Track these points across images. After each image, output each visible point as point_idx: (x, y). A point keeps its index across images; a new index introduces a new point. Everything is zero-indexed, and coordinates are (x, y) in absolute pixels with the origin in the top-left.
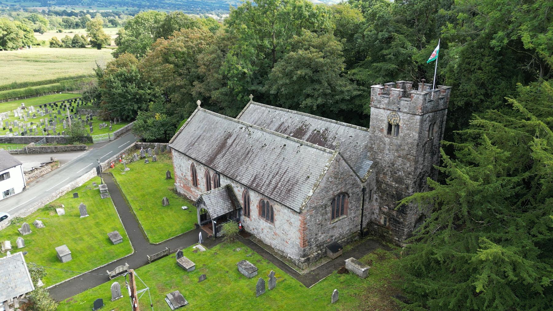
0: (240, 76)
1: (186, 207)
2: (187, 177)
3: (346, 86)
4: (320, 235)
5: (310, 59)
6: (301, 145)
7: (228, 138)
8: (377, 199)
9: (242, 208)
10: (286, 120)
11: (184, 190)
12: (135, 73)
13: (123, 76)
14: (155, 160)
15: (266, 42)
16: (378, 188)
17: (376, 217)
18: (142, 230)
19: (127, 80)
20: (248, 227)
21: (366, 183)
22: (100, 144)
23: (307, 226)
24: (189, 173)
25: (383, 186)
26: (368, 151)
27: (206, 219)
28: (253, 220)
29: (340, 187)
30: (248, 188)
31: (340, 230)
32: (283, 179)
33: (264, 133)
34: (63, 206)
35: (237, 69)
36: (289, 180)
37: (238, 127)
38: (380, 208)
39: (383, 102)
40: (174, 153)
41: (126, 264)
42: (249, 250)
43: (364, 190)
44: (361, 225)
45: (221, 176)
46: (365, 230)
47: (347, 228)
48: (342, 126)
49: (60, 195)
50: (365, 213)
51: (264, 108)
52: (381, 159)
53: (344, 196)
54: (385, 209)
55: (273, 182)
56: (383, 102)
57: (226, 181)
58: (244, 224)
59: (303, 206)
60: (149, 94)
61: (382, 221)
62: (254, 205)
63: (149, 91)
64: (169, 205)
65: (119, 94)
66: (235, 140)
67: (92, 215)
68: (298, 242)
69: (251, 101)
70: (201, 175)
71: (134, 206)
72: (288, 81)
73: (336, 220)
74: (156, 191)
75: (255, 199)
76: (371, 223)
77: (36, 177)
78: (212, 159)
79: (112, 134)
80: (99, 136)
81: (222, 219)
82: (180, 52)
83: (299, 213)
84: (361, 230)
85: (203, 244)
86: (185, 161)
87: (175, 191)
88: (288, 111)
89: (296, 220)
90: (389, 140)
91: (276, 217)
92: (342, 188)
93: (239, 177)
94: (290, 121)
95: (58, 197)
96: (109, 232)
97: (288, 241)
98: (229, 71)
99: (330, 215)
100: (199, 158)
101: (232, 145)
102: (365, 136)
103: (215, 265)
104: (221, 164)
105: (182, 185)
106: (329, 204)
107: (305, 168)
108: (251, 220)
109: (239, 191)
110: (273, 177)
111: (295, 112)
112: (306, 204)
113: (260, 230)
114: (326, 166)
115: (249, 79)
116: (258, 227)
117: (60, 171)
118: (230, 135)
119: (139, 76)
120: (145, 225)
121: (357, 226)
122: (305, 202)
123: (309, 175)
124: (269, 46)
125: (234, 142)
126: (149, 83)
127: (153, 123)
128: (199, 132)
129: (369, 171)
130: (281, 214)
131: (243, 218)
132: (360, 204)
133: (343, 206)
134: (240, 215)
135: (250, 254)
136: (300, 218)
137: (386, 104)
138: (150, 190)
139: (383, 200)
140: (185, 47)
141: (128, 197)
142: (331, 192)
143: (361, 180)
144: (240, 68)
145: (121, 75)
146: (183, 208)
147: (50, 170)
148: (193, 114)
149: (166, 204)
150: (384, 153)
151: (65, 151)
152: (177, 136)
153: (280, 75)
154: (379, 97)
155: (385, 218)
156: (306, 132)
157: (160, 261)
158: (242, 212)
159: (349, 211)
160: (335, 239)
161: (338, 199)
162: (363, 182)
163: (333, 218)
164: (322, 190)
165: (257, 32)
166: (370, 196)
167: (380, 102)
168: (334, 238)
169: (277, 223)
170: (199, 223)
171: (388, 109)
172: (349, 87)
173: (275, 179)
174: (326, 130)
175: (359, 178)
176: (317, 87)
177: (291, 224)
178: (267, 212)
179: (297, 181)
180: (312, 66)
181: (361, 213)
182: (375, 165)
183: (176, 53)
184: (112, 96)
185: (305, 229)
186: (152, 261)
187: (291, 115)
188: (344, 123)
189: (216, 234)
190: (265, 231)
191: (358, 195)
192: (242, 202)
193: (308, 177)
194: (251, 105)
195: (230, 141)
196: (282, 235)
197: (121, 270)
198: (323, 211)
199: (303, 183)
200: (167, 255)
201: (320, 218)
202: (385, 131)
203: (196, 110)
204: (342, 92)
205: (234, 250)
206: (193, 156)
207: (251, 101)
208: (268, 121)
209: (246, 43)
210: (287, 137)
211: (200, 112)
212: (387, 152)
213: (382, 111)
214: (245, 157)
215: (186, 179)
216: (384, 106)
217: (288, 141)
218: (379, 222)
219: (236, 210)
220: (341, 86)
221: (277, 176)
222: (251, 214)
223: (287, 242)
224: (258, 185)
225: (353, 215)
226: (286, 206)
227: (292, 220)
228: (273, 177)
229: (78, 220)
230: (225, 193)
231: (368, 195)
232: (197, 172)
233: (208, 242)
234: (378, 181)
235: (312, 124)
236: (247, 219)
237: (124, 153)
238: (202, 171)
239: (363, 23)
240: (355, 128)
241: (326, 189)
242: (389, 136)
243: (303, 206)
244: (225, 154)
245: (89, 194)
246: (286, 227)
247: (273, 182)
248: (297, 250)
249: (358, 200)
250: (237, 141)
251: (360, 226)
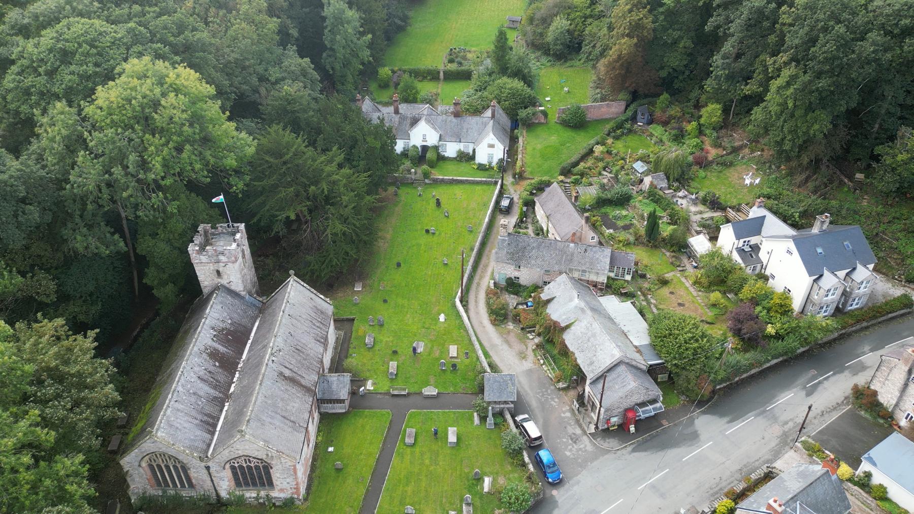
10: (195, 373)
51: (169, 411)
55: (318, 324)
94: (196, 369)
118: (281, 374)
156: (215, 349)
174: (213, 328)
195: (287, 373)
208: (193, 399)
224: (322, 338)
247: (318, 324)
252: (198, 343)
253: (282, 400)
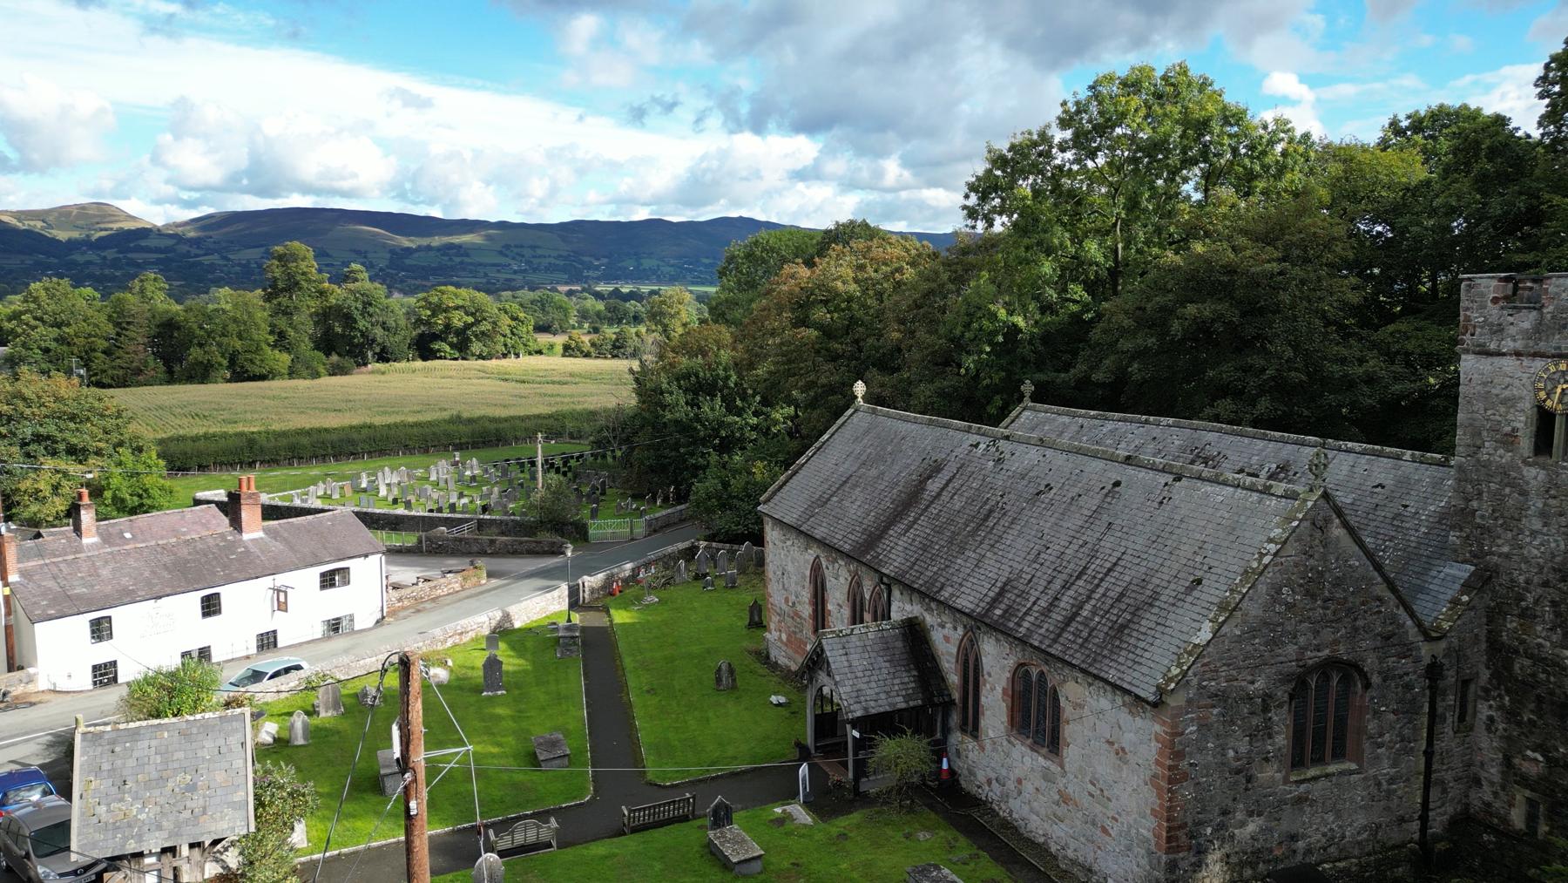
0: (1000, 339)
1: (782, 700)
2: (799, 608)
3: (1361, 361)
4: (1239, 816)
5: (1230, 270)
6: (1178, 478)
7: (929, 477)
8: (1491, 719)
9: (952, 702)
11: (790, 652)
12: (725, 370)
13: (693, 379)
14: (732, 585)
15: (1093, 248)
16: (1496, 675)
17: (1488, 797)
18: (634, 743)
19: (699, 387)
20: (972, 773)
21: (1443, 644)
22: (602, 545)
23: (1184, 764)
24: (806, 595)
25: (1521, 665)
26: (1453, 527)
27: (834, 735)
28: (988, 747)
29: (1327, 635)
30: (978, 623)
31: (1330, 817)
32: (1101, 590)
33: (1049, 452)
34: (450, 663)
35: (993, 316)
36: (1122, 595)
37: (966, 445)
38: (1507, 762)
39: (1512, 330)
40: (772, 534)
41: (553, 820)
42: (963, 841)
43: (1433, 671)
44: (1424, 819)
45: (896, 593)
46: (1441, 846)
47: (1361, 820)
48: (1342, 455)
49: (457, 639)
50: (1443, 773)
51: (1066, 419)
52: (1507, 556)
53: (1346, 680)
54: (1532, 763)
56: (1512, 330)
57: (908, 607)
58: (959, 765)
59: (1171, 680)
60: (754, 428)
61: (1517, 817)
62: (993, 689)
63: (755, 421)
64: (734, 687)
65: (677, 422)
66: (950, 481)
67: (517, 692)
68: (1149, 828)
69: (1027, 402)
70: (838, 594)
71: (635, 683)
72: (1151, 341)
73: (1312, 772)
74: (708, 651)
75: (997, 661)
76: (1464, 822)
77: (418, 600)
78: (874, 538)
79: (640, 526)
80: (603, 527)
81: (878, 724)
82: (838, 295)
83: (1155, 705)
84: (1423, 842)
85: (807, 804)
86: (797, 555)
87: (764, 657)
88: (1147, 422)
89: (1143, 737)
90: (1542, 475)
91: (1068, 731)
92: (1336, 642)
93: (950, 590)
95: (449, 644)
96: (540, 729)
98: (967, 326)
99: (1282, 740)
100: (837, 540)
101: (939, 495)
102: (1437, 484)
103: (833, 871)
104: (896, 554)
105: (784, 637)
106: (1281, 694)
107: (1186, 550)
108: (983, 748)
109: (947, 639)
110: (1066, 586)
111: (1171, 420)
112: (1185, 674)
113: (1011, 785)
114: (1270, 541)
115: (1026, 350)
116: (1004, 772)
117: (482, 593)
118: (937, 468)
119: (734, 378)
120: (646, 729)
121: (1402, 820)
122: (1179, 665)
123: (1199, 574)
124: (1100, 259)
125: (947, 485)
126: (758, 398)
127: (745, 489)
128: (848, 467)
129: (1455, 602)
130: (1089, 715)
131: (956, 738)
132: (1416, 729)
133: (1341, 723)
134: (946, 731)
135: (965, 854)
136: (1157, 728)
137: (1527, 335)
138: (695, 649)
139: (1519, 724)
140: (856, 281)
141: (628, 662)
142: (1291, 649)
143: (1419, 624)
144: (1002, 314)
145: (687, 376)
146: (774, 699)
147: (457, 587)
148: (840, 421)
149: (726, 681)
150: (1521, 532)
151: (514, 553)
152: (785, 483)
153: (1126, 322)
154: (1493, 311)
155: (1531, 803)
157: (657, 834)
158: (955, 719)
159: (1367, 745)
160: (1309, 851)
161: (1323, 688)
162: (1428, 638)
163: (1297, 762)
164: (1253, 632)
165: (1066, 219)
166: (1463, 707)
167: (1498, 330)
168: (1301, 844)
169: (1071, 753)
170: (809, 740)
171: (1535, 355)
172: (1374, 364)
173: (1071, 593)
175: (1412, 615)
176: (1258, 361)
177: (1121, 753)
178: (1038, 719)
179: (1155, 596)
180: (1239, 293)
181: (1422, 767)
182: (1483, 580)
183: (830, 299)
184: (658, 427)
185: (1175, 777)
186: (635, 830)
187: (1156, 431)
188: (1350, 444)
189: (857, 779)
190: (1028, 787)
191: (1408, 687)
192: (954, 679)
193: (1199, 582)
194: (1027, 413)
195: (933, 486)
196: (1086, 801)
197: (531, 836)
198: (1255, 721)
199: (1178, 600)
200: (684, 819)
201: (1244, 748)
202: (1526, 444)
203: (850, 411)
204: (1349, 384)
205: (908, 836)
206: (819, 533)
207: (1027, 402)
209: (1026, 241)
210: (1128, 458)
211: (860, 414)
212: (1537, 524)
213: (1509, 364)
214: (978, 529)
215: (797, 614)
216: (1519, 345)
217: (1130, 470)
218: (1505, 820)
219: (934, 705)
220: (1343, 361)
221: (1081, 583)
222: (982, 723)
223: (1104, 830)
225: (1386, 769)
226: (1106, 681)
227: (1127, 739)
228: (1066, 586)
229: (473, 699)
230: (899, 644)
231: (1451, 699)
232: (828, 585)
233: (826, 802)
234: (1495, 647)
235: (1228, 453)
236: (970, 744)
237: (656, 561)
238: (842, 580)
239: (1427, 183)
240: (1398, 458)
241: (1270, 632)
242: (1541, 459)
243: (1171, 680)
244: (914, 522)
245: (529, 644)
246: (1104, 767)
247: (1065, 602)
248: (1144, 862)
249: (1408, 710)
250: (956, 484)
251: (1415, 826)
252: (1232, 438)
253: (881, 475)
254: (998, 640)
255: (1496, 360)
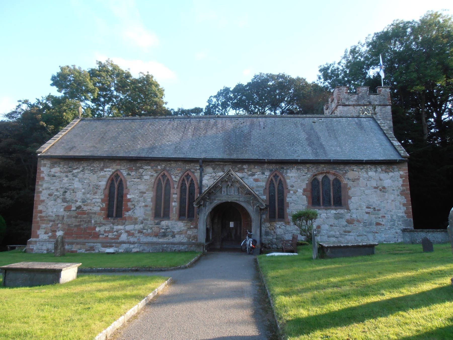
56: (352, 99)
97: (380, 221)
154: (346, 96)
213: (351, 108)
216: (354, 103)
254: (298, 169)
255: (348, 107)
